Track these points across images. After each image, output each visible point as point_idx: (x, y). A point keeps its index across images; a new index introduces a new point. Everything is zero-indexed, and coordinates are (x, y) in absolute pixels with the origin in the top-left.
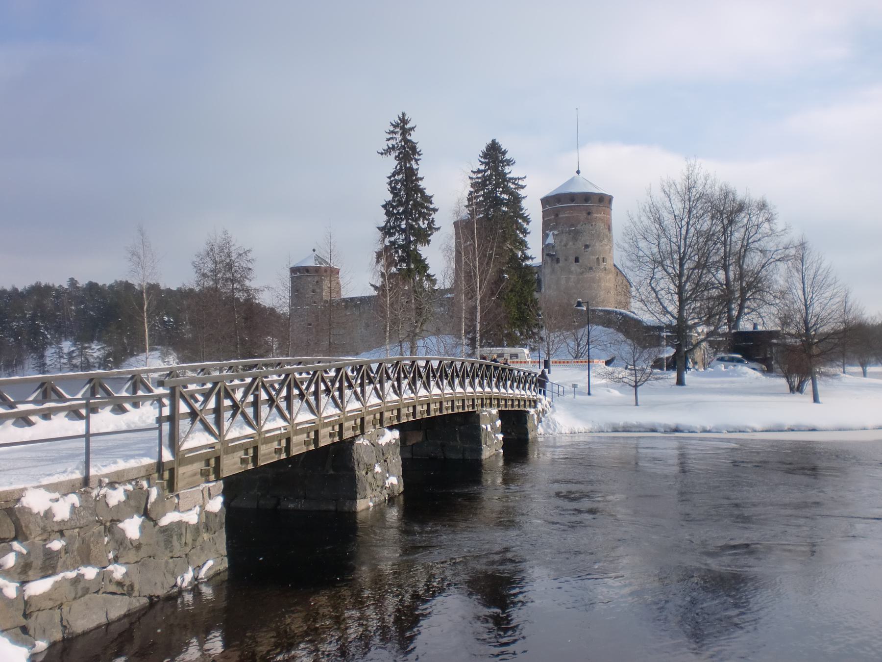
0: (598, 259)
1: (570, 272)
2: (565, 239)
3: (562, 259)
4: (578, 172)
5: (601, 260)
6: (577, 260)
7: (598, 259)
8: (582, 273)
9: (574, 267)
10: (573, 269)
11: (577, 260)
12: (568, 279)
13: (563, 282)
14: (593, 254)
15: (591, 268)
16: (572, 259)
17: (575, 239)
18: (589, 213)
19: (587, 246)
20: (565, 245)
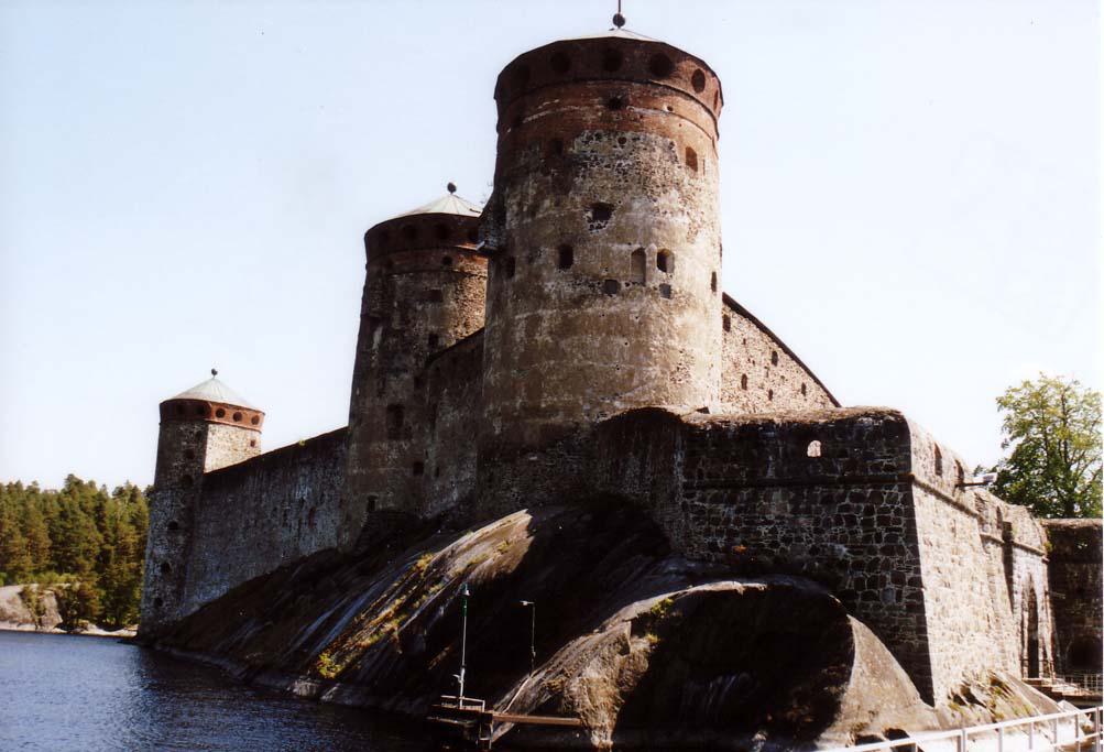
0: (640, 254)
1: (542, 299)
2: (532, 192)
3: (520, 255)
4: (619, 21)
5: (651, 259)
6: (565, 259)
7: (640, 254)
8: (578, 302)
9: (555, 284)
10: (549, 286)
11: (565, 259)
12: (535, 321)
13: (519, 335)
14: (620, 236)
15: (611, 287)
16: (548, 253)
17: (562, 187)
18: (615, 104)
19: (602, 212)
20: (533, 211)
